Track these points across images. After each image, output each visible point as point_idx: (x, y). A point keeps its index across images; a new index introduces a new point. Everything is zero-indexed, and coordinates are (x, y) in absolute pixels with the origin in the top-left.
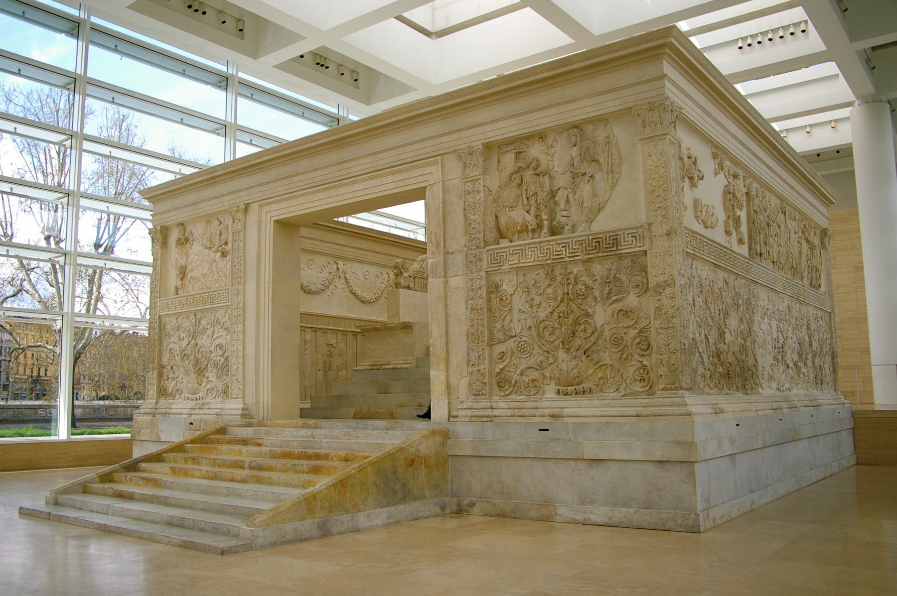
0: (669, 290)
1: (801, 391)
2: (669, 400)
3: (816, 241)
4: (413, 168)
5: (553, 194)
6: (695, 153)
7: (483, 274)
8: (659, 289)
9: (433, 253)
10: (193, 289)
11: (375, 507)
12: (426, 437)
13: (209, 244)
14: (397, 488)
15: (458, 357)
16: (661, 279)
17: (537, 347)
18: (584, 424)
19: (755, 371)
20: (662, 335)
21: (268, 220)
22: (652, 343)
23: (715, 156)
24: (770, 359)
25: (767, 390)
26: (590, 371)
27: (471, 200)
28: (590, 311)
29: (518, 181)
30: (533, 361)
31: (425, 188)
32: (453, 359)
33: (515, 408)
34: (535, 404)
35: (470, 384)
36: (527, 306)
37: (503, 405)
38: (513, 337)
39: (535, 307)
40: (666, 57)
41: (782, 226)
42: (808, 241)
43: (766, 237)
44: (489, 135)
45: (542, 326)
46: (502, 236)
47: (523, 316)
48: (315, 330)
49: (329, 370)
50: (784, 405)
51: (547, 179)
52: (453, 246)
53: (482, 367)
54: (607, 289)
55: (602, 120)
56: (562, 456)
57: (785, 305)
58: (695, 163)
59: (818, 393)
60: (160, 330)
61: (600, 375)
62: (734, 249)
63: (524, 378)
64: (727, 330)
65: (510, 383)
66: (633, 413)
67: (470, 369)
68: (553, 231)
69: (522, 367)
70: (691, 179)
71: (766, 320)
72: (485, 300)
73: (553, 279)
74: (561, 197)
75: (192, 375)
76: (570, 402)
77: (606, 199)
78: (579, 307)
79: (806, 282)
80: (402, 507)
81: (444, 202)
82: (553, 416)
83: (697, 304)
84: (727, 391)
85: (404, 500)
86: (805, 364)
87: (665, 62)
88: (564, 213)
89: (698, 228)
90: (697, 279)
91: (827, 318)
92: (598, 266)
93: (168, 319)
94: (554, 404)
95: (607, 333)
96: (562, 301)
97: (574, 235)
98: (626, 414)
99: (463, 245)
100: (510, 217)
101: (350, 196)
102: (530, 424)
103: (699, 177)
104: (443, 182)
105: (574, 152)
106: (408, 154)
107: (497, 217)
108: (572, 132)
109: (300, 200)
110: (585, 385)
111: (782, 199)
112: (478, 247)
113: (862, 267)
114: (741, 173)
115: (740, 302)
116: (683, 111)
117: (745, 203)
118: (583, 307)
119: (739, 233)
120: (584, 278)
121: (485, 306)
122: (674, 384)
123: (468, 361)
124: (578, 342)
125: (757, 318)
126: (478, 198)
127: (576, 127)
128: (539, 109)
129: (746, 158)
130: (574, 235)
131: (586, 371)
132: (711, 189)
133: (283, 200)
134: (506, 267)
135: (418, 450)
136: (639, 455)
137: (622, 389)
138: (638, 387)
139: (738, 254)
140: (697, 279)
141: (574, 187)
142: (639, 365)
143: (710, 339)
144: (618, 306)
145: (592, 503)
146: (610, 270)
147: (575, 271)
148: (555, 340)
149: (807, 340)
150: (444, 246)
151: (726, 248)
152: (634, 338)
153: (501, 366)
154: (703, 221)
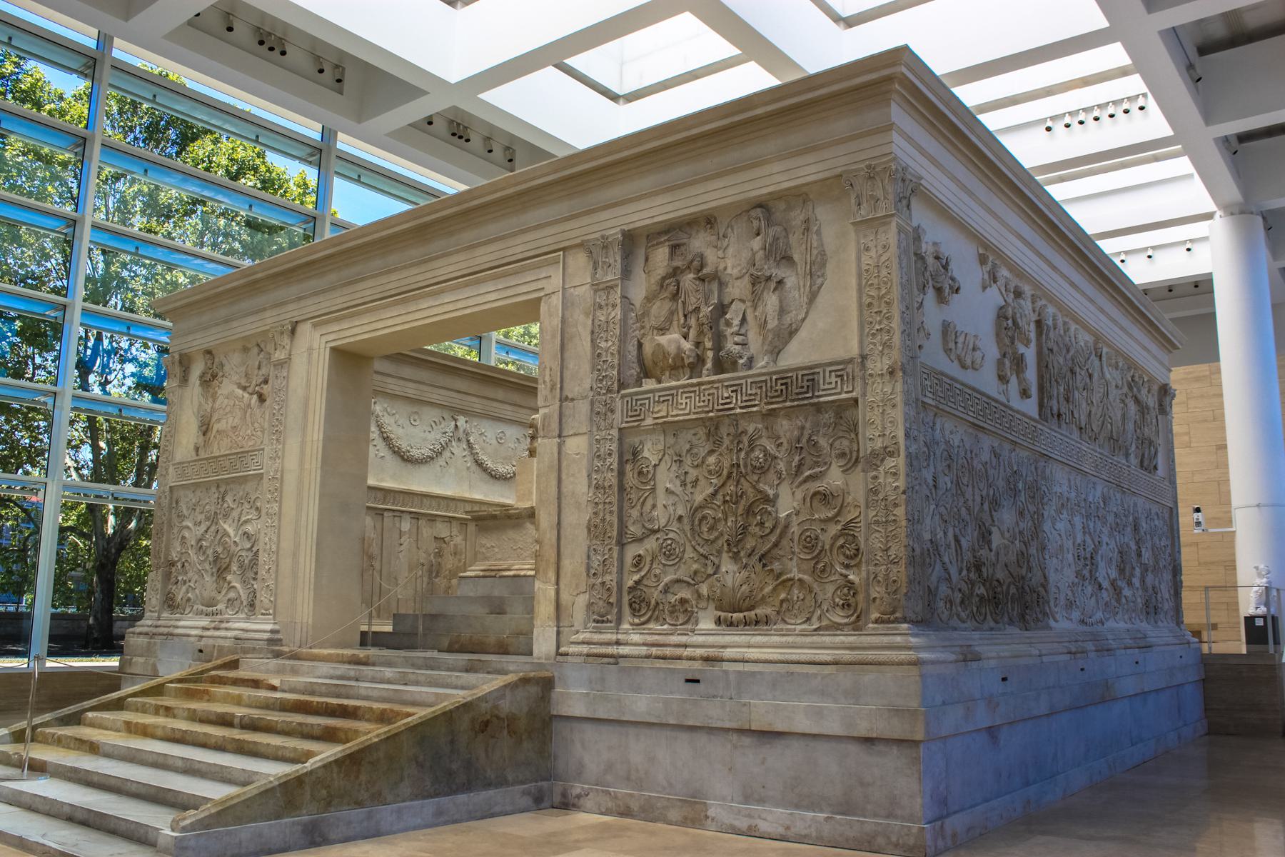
0: (890, 462)
1: (1122, 625)
2: (885, 639)
3: (1151, 401)
5: (722, 309)
6: (945, 251)
7: (615, 432)
8: (875, 459)
9: (546, 399)
10: (220, 448)
11: (415, 797)
12: (512, 686)
13: (244, 383)
14: (454, 766)
15: (573, 562)
16: (879, 444)
17: (689, 549)
18: (753, 674)
19: (1042, 592)
20: (877, 535)
21: (323, 346)
22: (862, 546)
23: (983, 260)
24: (1069, 574)
25: (1063, 623)
26: (768, 589)
27: (602, 318)
28: (771, 492)
29: (672, 288)
30: (683, 573)
31: (539, 299)
32: (566, 563)
33: (653, 645)
34: (683, 639)
35: (590, 605)
36: (678, 483)
37: (636, 638)
38: (655, 532)
39: (689, 486)
40: (894, 96)
41: (1096, 376)
42: (1137, 401)
43: (1068, 390)
45: (699, 515)
46: (646, 373)
47: (672, 499)
48: (417, 516)
49: (437, 576)
50: (1090, 646)
51: (715, 286)
52: (573, 389)
53: (607, 578)
54: (797, 458)
55: (799, 196)
56: (719, 724)
57: (1098, 493)
58: (945, 267)
59: (1149, 627)
60: (171, 508)
61: (783, 596)
62: (1011, 404)
63: (670, 596)
64: (994, 529)
65: (648, 604)
66: (829, 658)
67: (592, 581)
68: (720, 367)
69: (667, 579)
70: (939, 290)
71: (1065, 515)
72: (615, 474)
73: (718, 443)
74: (733, 315)
75: (207, 578)
76: (736, 639)
77: (800, 317)
78: (754, 487)
79: (1134, 461)
80: (462, 798)
81: (564, 321)
82: (707, 659)
83: (941, 484)
84: (992, 624)
85: (467, 787)
86: (1130, 584)
87: (893, 105)
88: (737, 339)
89: (953, 369)
90: (943, 446)
91: (1167, 516)
92: (785, 422)
93: (182, 493)
94: (711, 639)
95: (795, 529)
96: (729, 476)
97: (750, 372)
98: (817, 658)
99: (588, 386)
100: (659, 345)
101: (436, 311)
102: (672, 671)
103: (951, 287)
104: (564, 289)
105: (757, 243)
106: (518, 247)
107: (640, 345)
108: (753, 213)
110: (760, 611)
111: (1098, 337)
112: (609, 391)
113: (1225, 447)
114: (1027, 290)
115: (1020, 485)
116: (923, 182)
117: (1033, 336)
118: (761, 486)
119: (1021, 381)
120: (765, 442)
121: (615, 481)
122: (893, 613)
123: (588, 568)
124: (750, 543)
125: (1049, 511)
126: (613, 314)
127: (760, 206)
128: (706, 179)
129: (1035, 268)
130: (750, 372)
131: (762, 589)
132: (975, 309)
133: (343, 318)
134: (649, 421)
135: (496, 707)
136: (833, 726)
137: (814, 619)
138: (838, 617)
139: (1018, 412)
140: (943, 446)
141: (756, 299)
142: (841, 581)
143: (964, 542)
144: (814, 486)
145: (761, 801)
146: (803, 428)
147: (751, 429)
148: (717, 538)
149: (1134, 547)
150: (561, 388)
151: (996, 401)
152: (835, 538)
153: (636, 577)
154: (959, 358)
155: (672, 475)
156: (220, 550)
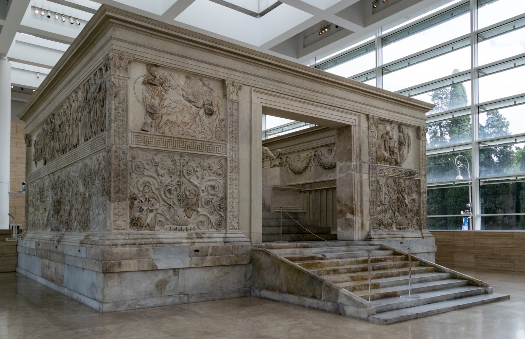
4: (348, 113)
13: (191, 98)
30: (389, 216)
44: (380, 114)
109: (284, 101)
155: (386, 190)
156: (188, 193)
